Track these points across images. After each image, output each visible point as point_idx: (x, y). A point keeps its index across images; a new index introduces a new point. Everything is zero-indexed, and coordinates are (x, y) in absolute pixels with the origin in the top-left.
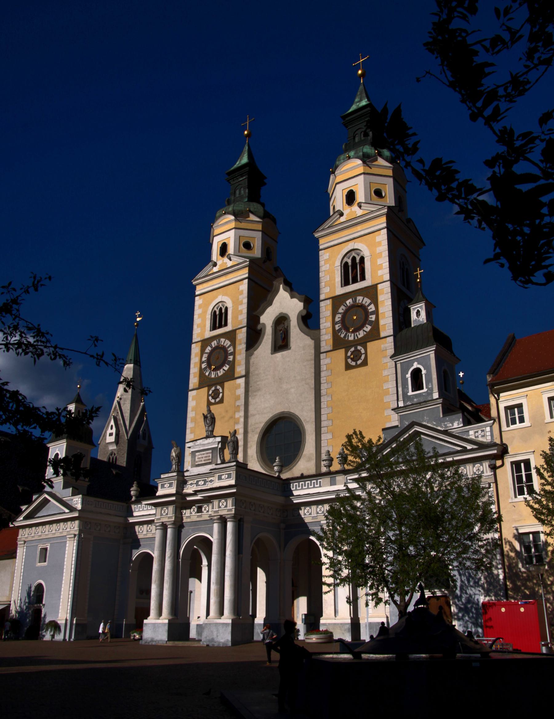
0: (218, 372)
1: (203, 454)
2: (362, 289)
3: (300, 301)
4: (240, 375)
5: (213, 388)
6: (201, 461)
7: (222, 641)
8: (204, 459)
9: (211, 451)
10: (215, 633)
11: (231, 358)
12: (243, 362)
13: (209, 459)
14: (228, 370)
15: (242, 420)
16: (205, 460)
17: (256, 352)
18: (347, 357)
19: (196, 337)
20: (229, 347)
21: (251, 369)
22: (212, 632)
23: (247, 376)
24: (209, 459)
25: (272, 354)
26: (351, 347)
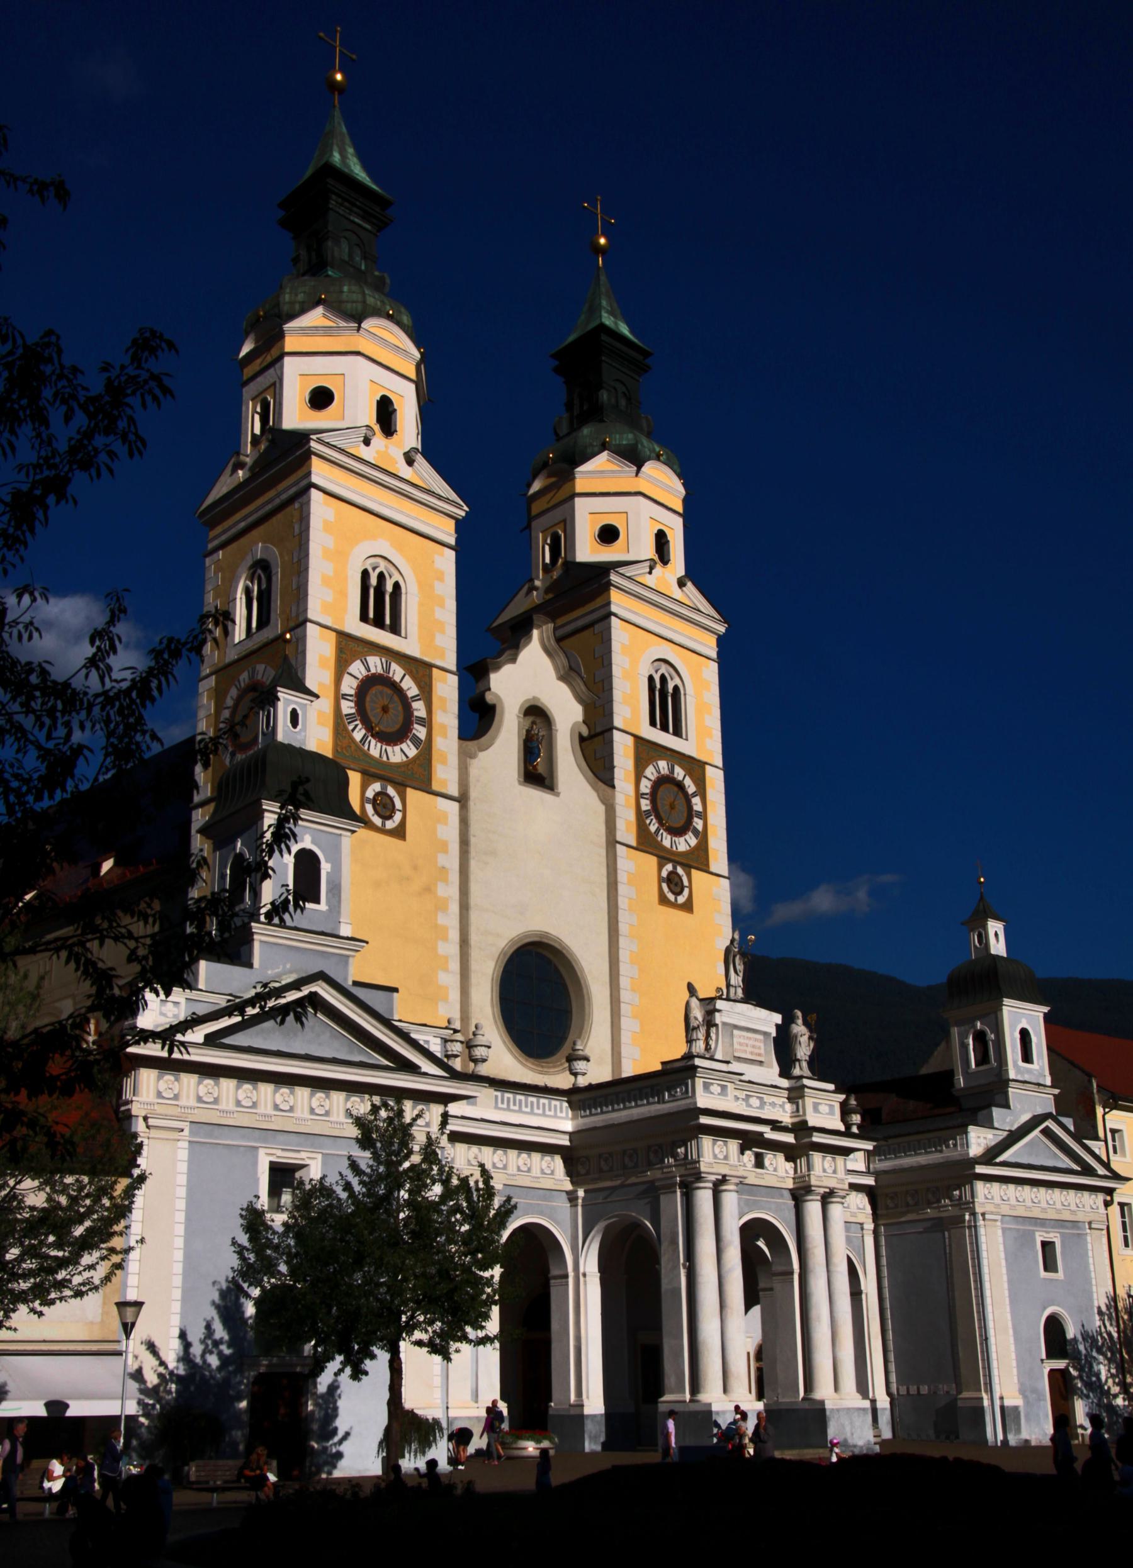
0: (389, 749)
1: (750, 1038)
2: (683, 755)
3: (579, 699)
4: (443, 791)
5: (376, 787)
6: (745, 1051)
7: (861, 1443)
8: (749, 1049)
9: (761, 1037)
10: (848, 1429)
11: (420, 732)
12: (453, 759)
13: (760, 1055)
14: (416, 757)
15: (454, 908)
16: (752, 1053)
17: (482, 755)
18: (661, 880)
19: (315, 609)
20: (415, 698)
21: (473, 794)
22: (843, 1426)
23: (463, 799)
24: (760, 1055)
25: (520, 783)
26: (670, 860)
